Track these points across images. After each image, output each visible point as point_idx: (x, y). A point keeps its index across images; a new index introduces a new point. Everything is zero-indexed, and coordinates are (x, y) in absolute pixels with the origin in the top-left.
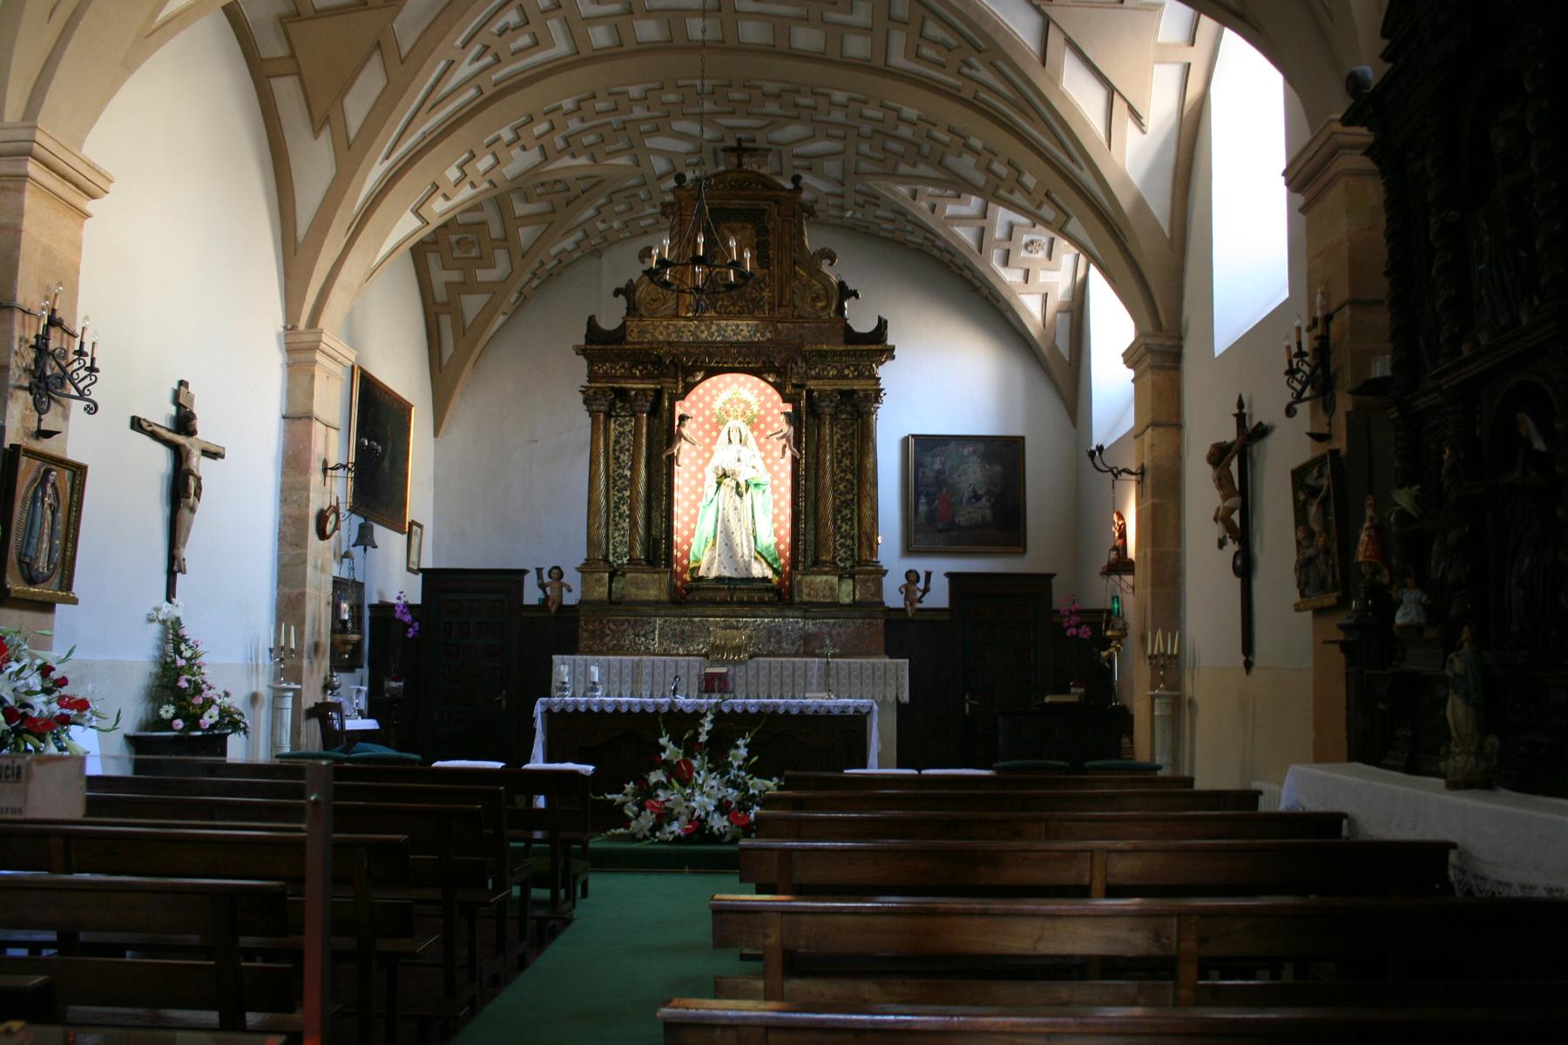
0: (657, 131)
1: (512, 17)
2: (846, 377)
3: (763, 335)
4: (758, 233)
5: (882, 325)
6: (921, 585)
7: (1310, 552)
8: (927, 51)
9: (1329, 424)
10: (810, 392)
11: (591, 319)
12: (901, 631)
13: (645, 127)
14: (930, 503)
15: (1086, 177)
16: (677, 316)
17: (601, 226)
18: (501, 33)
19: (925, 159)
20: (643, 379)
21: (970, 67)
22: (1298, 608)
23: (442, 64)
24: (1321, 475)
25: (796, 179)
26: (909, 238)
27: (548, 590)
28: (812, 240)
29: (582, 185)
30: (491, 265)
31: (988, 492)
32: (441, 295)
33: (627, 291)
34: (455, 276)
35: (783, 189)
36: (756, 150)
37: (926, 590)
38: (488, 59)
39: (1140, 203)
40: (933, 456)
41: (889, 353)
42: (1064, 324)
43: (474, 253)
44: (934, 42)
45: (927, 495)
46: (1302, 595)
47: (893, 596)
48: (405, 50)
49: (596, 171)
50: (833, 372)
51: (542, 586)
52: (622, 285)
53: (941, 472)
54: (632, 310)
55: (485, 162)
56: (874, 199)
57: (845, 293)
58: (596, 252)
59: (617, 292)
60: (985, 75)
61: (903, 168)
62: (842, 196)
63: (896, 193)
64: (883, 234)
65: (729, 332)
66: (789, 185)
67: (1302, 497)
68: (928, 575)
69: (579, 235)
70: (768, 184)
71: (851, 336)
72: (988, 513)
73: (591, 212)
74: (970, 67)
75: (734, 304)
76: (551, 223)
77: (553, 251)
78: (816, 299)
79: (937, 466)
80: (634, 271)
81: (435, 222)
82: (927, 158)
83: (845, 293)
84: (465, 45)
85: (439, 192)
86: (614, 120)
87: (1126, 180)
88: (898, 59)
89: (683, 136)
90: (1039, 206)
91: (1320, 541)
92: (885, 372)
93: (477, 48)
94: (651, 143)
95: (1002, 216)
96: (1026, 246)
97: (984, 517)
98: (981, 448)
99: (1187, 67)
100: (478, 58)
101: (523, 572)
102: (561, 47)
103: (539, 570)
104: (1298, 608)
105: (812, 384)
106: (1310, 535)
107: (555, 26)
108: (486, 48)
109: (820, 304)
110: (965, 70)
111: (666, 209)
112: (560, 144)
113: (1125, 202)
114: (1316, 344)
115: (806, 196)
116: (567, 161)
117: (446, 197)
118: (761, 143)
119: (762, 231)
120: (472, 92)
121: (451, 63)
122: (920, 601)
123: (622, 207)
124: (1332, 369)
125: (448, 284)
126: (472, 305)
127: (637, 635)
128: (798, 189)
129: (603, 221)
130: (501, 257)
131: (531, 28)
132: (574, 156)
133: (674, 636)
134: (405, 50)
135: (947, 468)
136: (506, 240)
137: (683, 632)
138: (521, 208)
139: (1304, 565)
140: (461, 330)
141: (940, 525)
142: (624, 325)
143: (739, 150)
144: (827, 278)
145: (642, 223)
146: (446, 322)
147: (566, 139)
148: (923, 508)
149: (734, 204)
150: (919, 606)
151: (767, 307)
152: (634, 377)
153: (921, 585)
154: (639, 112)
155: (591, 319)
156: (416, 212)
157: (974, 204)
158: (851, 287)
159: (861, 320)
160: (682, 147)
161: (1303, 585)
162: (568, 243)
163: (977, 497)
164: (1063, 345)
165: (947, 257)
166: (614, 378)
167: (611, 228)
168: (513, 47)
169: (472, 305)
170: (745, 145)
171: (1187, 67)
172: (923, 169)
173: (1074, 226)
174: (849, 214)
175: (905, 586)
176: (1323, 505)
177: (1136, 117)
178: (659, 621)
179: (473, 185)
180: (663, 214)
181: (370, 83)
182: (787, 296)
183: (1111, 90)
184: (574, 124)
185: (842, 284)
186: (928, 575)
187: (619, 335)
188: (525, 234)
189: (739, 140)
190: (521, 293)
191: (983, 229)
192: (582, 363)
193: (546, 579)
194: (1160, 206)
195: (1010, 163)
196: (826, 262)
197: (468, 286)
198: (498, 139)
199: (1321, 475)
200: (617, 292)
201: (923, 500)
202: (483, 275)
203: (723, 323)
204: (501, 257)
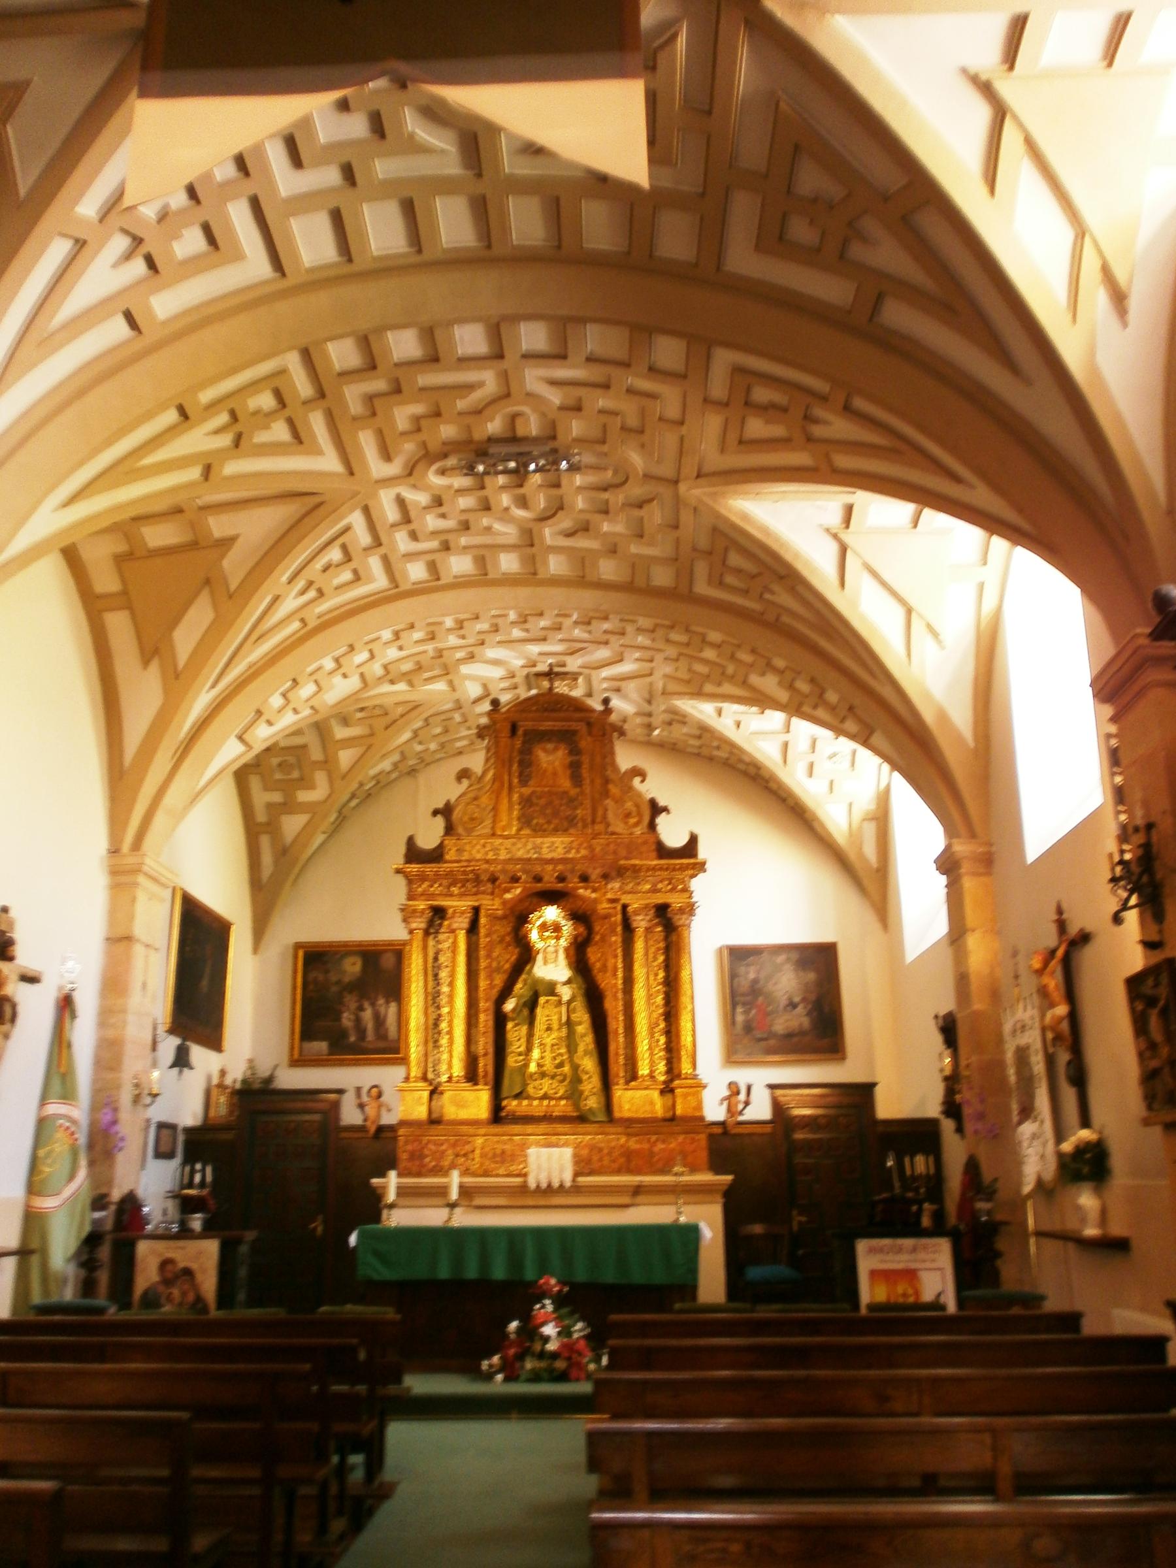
0: (471, 657)
1: (335, 554)
2: (659, 891)
3: (578, 851)
4: (571, 753)
5: (693, 840)
6: (742, 1097)
7: (1154, 1064)
8: (730, 579)
9: (1160, 932)
10: (625, 907)
11: (411, 841)
12: (726, 1145)
13: (460, 655)
14: (746, 1012)
15: (887, 692)
16: (494, 835)
17: (419, 748)
18: (326, 569)
19: (731, 679)
20: (462, 895)
21: (773, 593)
22: (1146, 1122)
23: (268, 599)
24: (1156, 985)
25: (606, 701)
26: (716, 753)
27: (367, 1108)
28: (625, 758)
29: (400, 710)
30: (312, 787)
31: (804, 1000)
32: (261, 817)
33: (446, 812)
34: (276, 797)
35: (593, 711)
36: (566, 674)
37: (747, 1103)
38: (312, 594)
39: (943, 716)
40: (748, 965)
41: (701, 867)
42: (870, 831)
43: (295, 774)
44: (738, 571)
45: (744, 1004)
46: (1150, 1107)
47: (714, 1111)
48: (233, 587)
49: (415, 696)
50: (648, 887)
51: (361, 1106)
52: (440, 805)
53: (755, 981)
54: (449, 829)
55: (307, 690)
56: (677, 718)
57: (656, 809)
58: (412, 772)
59: (436, 813)
60: (784, 598)
61: (709, 688)
62: (650, 715)
63: (701, 712)
64: (689, 750)
65: (545, 851)
66: (599, 707)
67: (1140, 1007)
68: (749, 1088)
69: (396, 757)
70: (577, 707)
71: (663, 851)
72: (806, 1022)
73: (407, 735)
74: (773, 593)
75: (549, 822)
76: (369, 747)
77: (372, 772)
78: (628, 815)
79: (752, 976)
80: (452, 791)
81: (258, 747)
82: (733, 677)
83: (656, 809)
84: (290, 581)
85: (264, 718)
86: (430, 647)
87: (928, 696)
88: (702, 587)
89: (496, 662)
90: (843, 720)
91: (1165, 1051)
92: (698, 885)
93: (301, 584)
94: (465, 669)
95: (803, 729)
96: (830, 757)
97: (801, 1025)
98: (795, 956)
99: (981, 586)
100: (303, 592)
101: (341, 1092)
102: (379, 581)
103: (358, 1090)
104: (1146, 1122)
105: (625, 899)
106: (1152, 1046)
107: (374, 563)
108: (310, 584)
109: (632, 821)
110: (767, 596)
111: (482, 732)
112: (377, 669)
113: (928, 716)
114: (1140, 852)
115: (613, 718)
116: (386, 688)
117: (270, 723)
118: (573, 664)
119: (574, 751)
120: (296, 625)
121: (276, 599)
122: (741, 1113)
123: (438, 730)
124: (1159, 876)
125: (270, 806)
126: (292, 825)
127: (457, 1155)
128: (608, 711)
129: (420, 743)
130: (321, 778)
131: (353, 565)
132: (392, 682)
133: (495, 1156)
134: (233, 587)
135: (762, 975)
136: (328, 763)
137: (503, 1152)
138: (341, 733)
139: (1149, 1078)
140: (283, 853)
141: (758, 1034)
142: (441, 846)
143: (550, 674)
144: (639, 795)
145: (459, 744)
146: (265, 841)
147: (385, 667)
148: (740, 1018)
149: (547, 725)
150: (741, 1118)
151: (580, 825)
152: (452, 895)
153: (742, 1097)
154: (453, 640)
155: (411, 841)
156: (240, 738)
157: (776, 718)
158: (662, 802)
159: (672, 833)
160: (497, 673)
161: (1150, 1099)
162: (386, 765)
163: (792, 1005)
164: (870, 851)
165: (752, 771)
166: (432, 896)
167: (427, 750)
168: (336, 582)
169: (292, 825)
170: (556, 669)
171: (981, 586)
172: (727, 688)
173: (877, 739)
174: (656, 732)
175: (728, 1098)
176: (1164, 1013)
177: (934, 633)
178: (479, 1141)
179: (295, 711)
180: (480, 736)
181: (199, 616)
182: (600, 813)
183: (909, 611)
184: (393, 653)
185: (653, 803)
186: (749, 1088)
187: (436, 855)
188: (346, 757)
189: (551, 665)
190: (340, 812)
191: (786, 745)
192: (401, 881)
193: (365, 1099)
194: (961, 717)
195: (812, 680)
196: (637, 781)
197: (288, 806)
198: (319, 669)
199: (1156, 985)
200: (436, 813)
201: (739, 1010)
202: (304, 796)
203: (539, 840)
204: (321, 778)
